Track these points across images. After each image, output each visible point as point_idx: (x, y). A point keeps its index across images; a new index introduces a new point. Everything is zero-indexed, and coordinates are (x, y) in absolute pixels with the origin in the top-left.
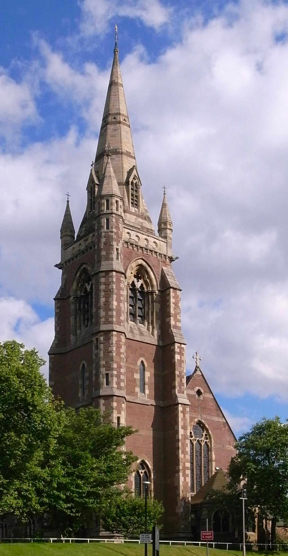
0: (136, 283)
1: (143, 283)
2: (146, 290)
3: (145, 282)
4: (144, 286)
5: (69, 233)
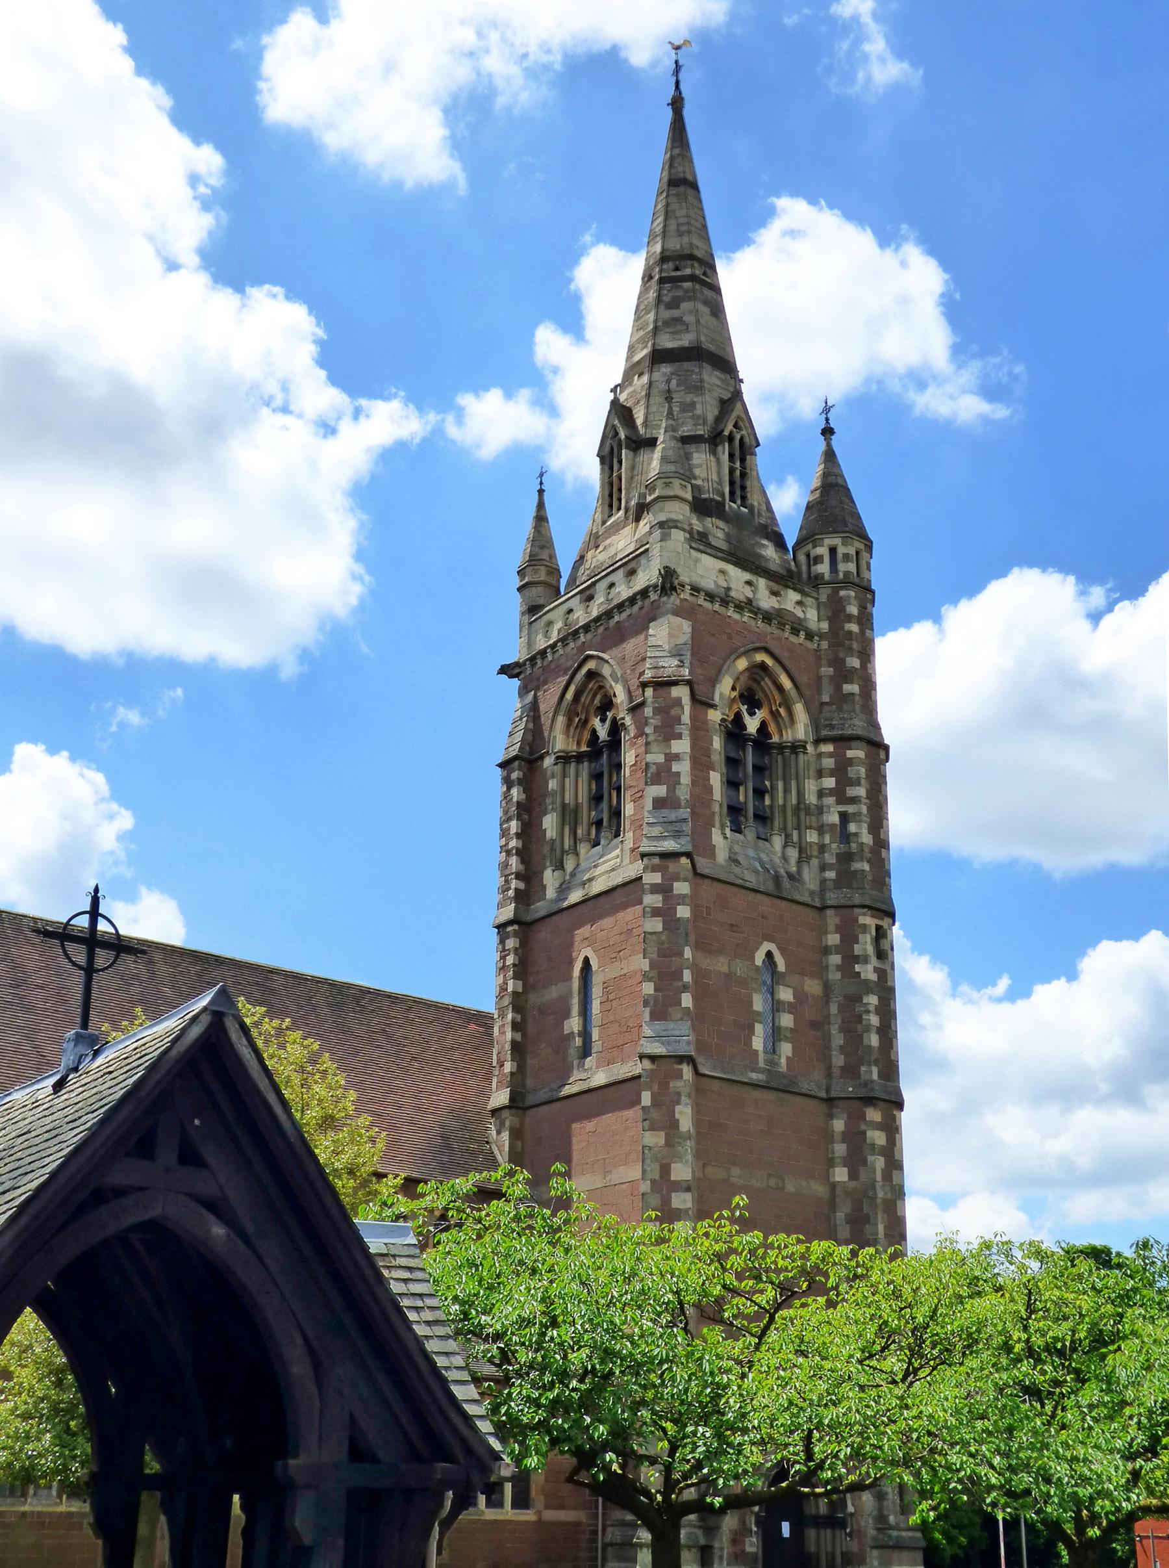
0: (747, 720)
1: (769, 718)
2: (775, 739)
3: (775, 715)
4: (772, 728)
5: (542, 576)
